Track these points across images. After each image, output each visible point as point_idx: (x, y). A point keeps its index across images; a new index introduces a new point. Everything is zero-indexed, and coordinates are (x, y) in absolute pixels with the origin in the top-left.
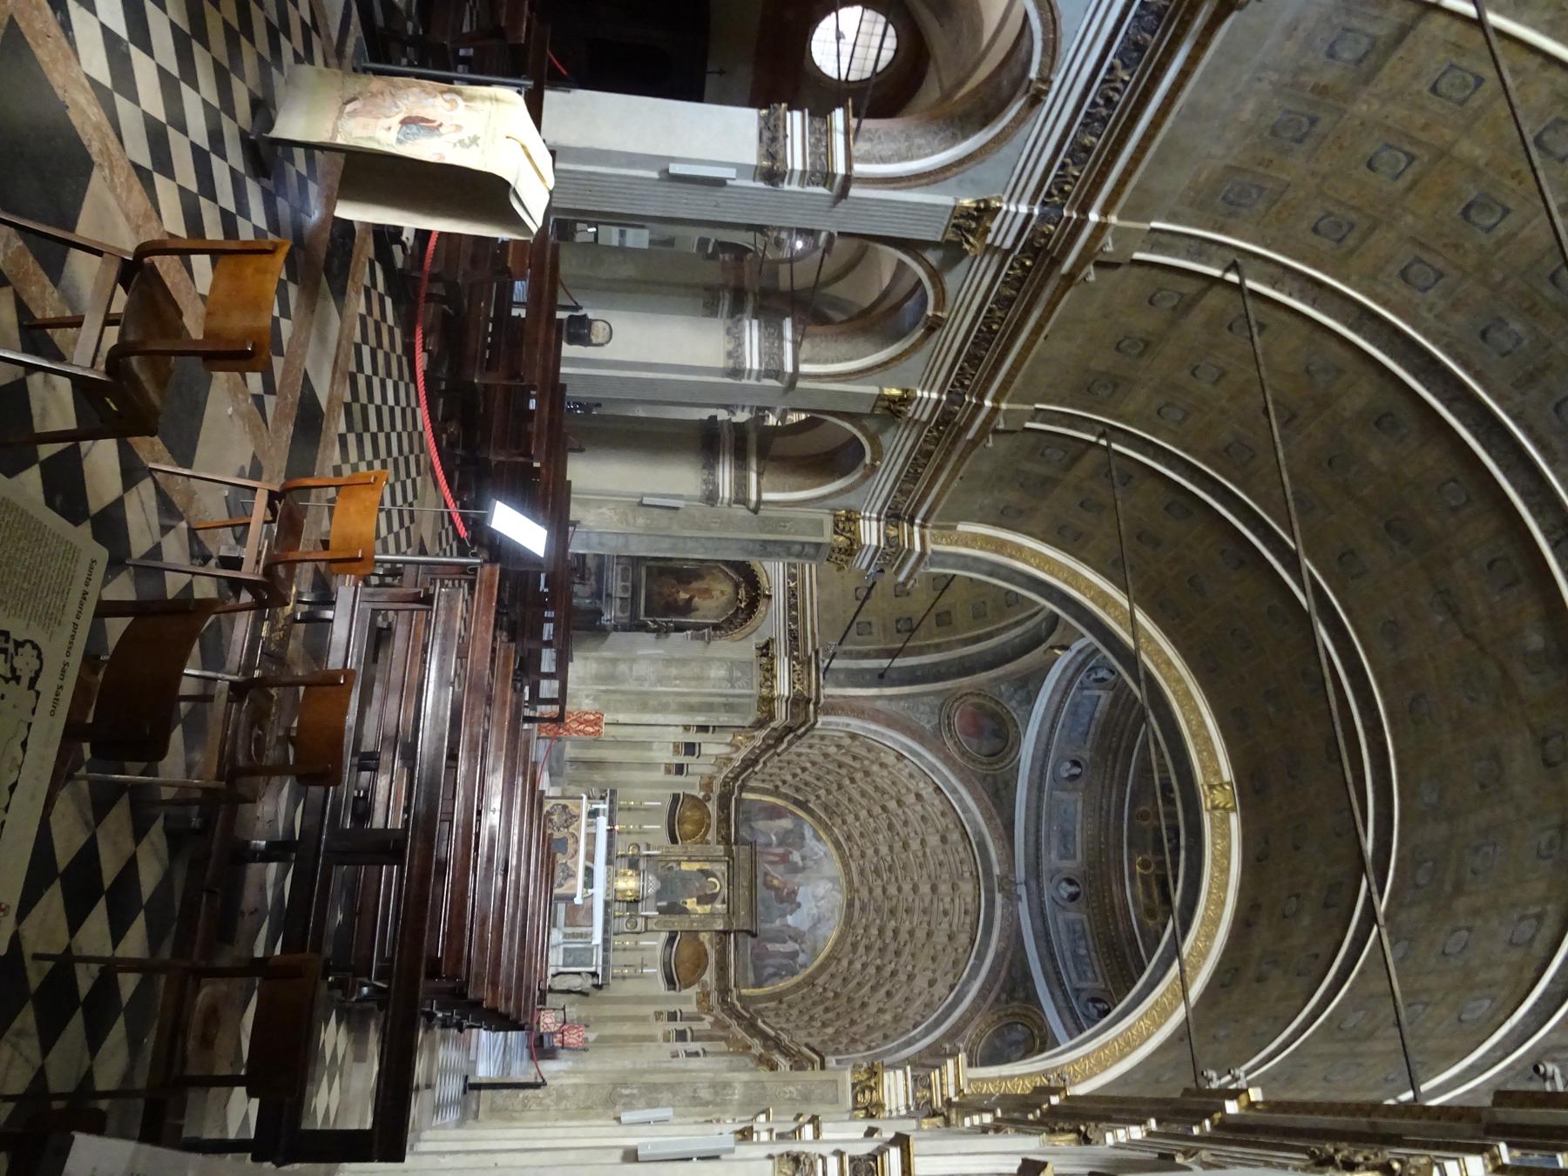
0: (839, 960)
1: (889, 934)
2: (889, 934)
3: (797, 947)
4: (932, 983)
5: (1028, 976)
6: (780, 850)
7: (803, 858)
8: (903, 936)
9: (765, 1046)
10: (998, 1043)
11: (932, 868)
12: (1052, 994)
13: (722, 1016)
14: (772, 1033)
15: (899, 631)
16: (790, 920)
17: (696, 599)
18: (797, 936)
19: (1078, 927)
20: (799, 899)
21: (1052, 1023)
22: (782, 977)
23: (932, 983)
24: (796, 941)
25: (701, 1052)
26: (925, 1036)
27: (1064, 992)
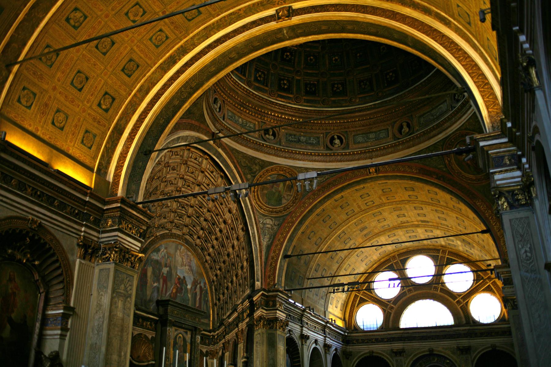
0: (206, 261)
1: (204, 223)
2: (204, 223)
3: (198, 286)
4: (230, 211)
5: (253, 159)
6: (161, 281)
7: (166, 266)
8: (208, 215)
9: (243, 320)
10: (266, 192)
11: (191, 179)
12: (267, 153)
13: (221, 344)
14: (236, 315)
15: (106, 110)
16: (189, 287)
17: (13, 316)
18: (195, 283)
19: (230, 114)
20: (182, 277)
21: (284, 163)
22: (208, 301)
23: (230, 211)
24: (197, 286)
25: (244, 360)
26: (253, 228)
27: (267, 146)
